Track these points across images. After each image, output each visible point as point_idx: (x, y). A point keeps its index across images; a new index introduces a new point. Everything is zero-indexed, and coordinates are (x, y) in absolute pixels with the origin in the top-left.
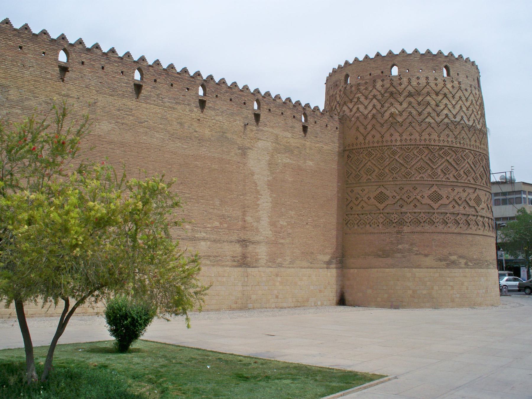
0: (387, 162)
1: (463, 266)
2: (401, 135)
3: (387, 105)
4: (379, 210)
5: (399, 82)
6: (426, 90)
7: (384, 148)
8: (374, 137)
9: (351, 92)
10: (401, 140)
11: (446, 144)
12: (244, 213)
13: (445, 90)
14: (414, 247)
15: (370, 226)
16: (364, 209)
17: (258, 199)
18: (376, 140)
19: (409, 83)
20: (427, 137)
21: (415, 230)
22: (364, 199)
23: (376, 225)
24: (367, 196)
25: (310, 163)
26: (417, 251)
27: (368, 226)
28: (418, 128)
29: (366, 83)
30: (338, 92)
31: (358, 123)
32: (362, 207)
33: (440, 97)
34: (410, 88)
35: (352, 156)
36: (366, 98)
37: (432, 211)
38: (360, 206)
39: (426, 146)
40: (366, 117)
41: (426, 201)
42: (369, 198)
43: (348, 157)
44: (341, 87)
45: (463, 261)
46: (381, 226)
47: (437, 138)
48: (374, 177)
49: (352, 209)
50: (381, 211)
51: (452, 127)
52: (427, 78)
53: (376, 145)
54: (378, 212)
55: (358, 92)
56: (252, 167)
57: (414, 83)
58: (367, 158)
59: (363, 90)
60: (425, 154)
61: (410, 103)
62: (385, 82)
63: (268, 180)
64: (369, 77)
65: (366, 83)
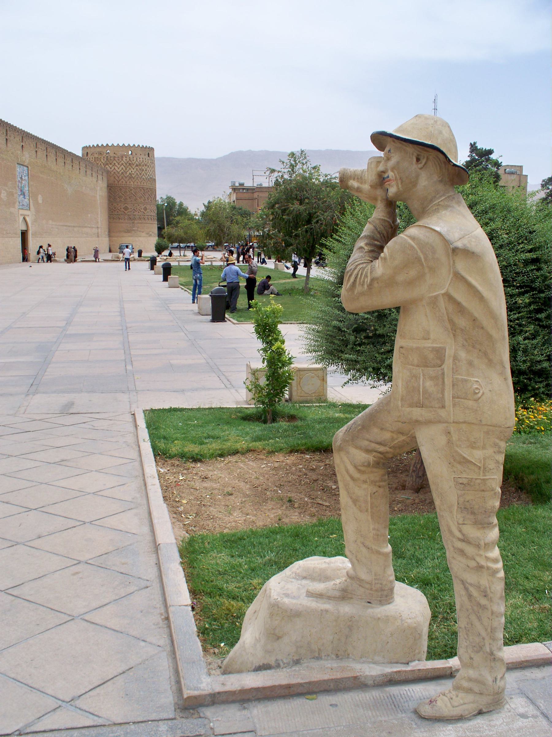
2: (134, 183)
3: (128, 169)
8: (122, 182)
13: (148, 164)
30: (102, 157)
31: (115, 175)
32: (118, 212)
33: (147, 167)
34: (137, 162)
36: (119, 164)
40: (119, 173)
41: (143, 210)
42: (121, 208)
43: (110, 189)
44: (104, 156)
45: (153, 234)
51: (150, 180)
53: (123, 186)
57: (138, 161)
61: (137, 169)
65: (118, 157)
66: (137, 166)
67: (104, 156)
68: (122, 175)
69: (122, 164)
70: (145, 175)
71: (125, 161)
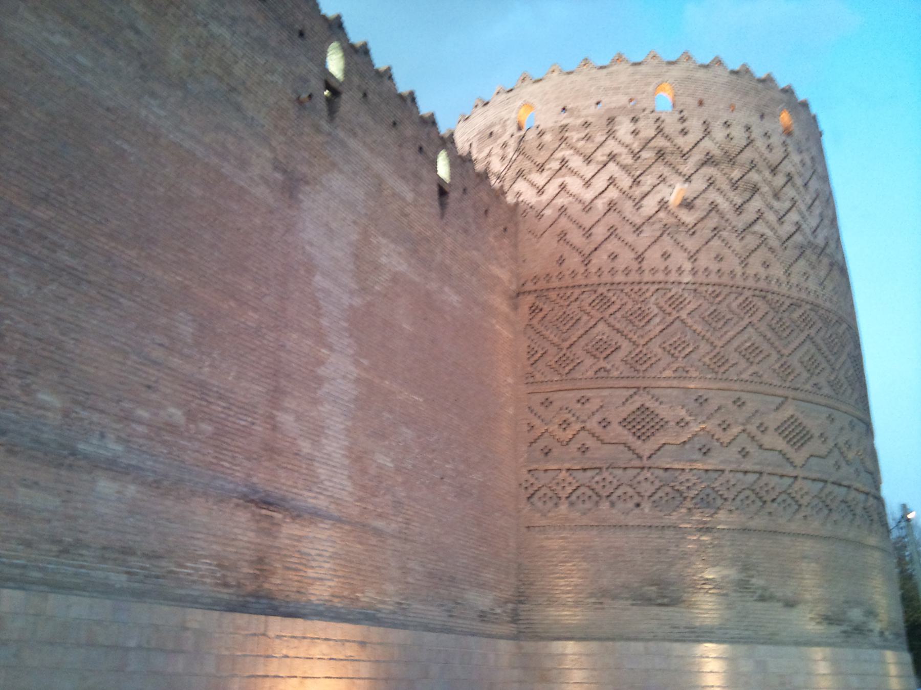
0: (655, 327)
1: (876, 639)
2: (693, 258)
3: (648, 180)
4: (640, 457)
5: (680, 127)
6: (748, 155)
7: (645, 288)
9: (541, 147)
10: (694, 272)
11: (803, 296)
12: (276, 396)
14: (752, 576)
15: (613, 504)
16: (588, 454)
17: (321, 362)
18: (620, 264)
19: (707, 132)
20: (763, 272)
21: (752, 524)
22: (588, 425)
23: (630, 505)
24: (598, 417)
25: (454, 299)
26: (765, 589)
27: (605, 505)
28: (737, 244)
29: (586, 124)
30: (497, 150)
32: (584, 450)
35: (546, 308)
36: (588, 160)
37: (789, 470)
38: (574, 446)
39: (757, 293)
42: (605, 423)
43: (534, 310)
44: (505, 137)
46: (646, 507)
47: (783, 278)
48: (618, 363)
49: (546, 454)
50: (645, 462)
52: (748, 128)
53: (620, 278)
54: (637, 463)
55: (563, 145)
56: (311, 244)
57: (719, 133)
58: (593, 312)
59: (578, 140)
60: (760, 314)
61: (711, 182)
62: (641, 124)
63: (351, 306)
64: (593, 110)
66: (709, 160)
67: (505, 137)
68: (612, 218)
69: (612, 157)
70: (771, 217)
71: (628, 139)
